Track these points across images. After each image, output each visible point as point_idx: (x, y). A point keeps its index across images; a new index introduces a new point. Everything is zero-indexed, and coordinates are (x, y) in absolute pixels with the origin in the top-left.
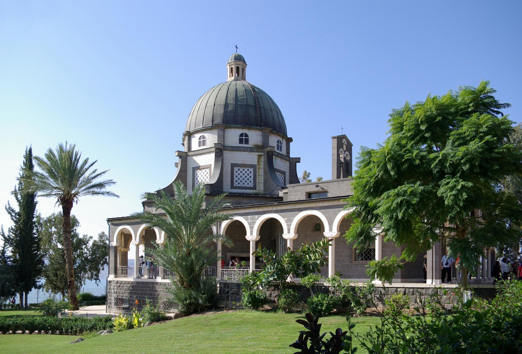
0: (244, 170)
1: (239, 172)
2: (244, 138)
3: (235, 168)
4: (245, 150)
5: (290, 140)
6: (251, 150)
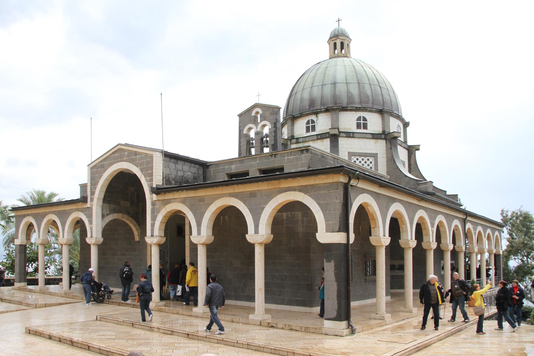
4: (364, 136)
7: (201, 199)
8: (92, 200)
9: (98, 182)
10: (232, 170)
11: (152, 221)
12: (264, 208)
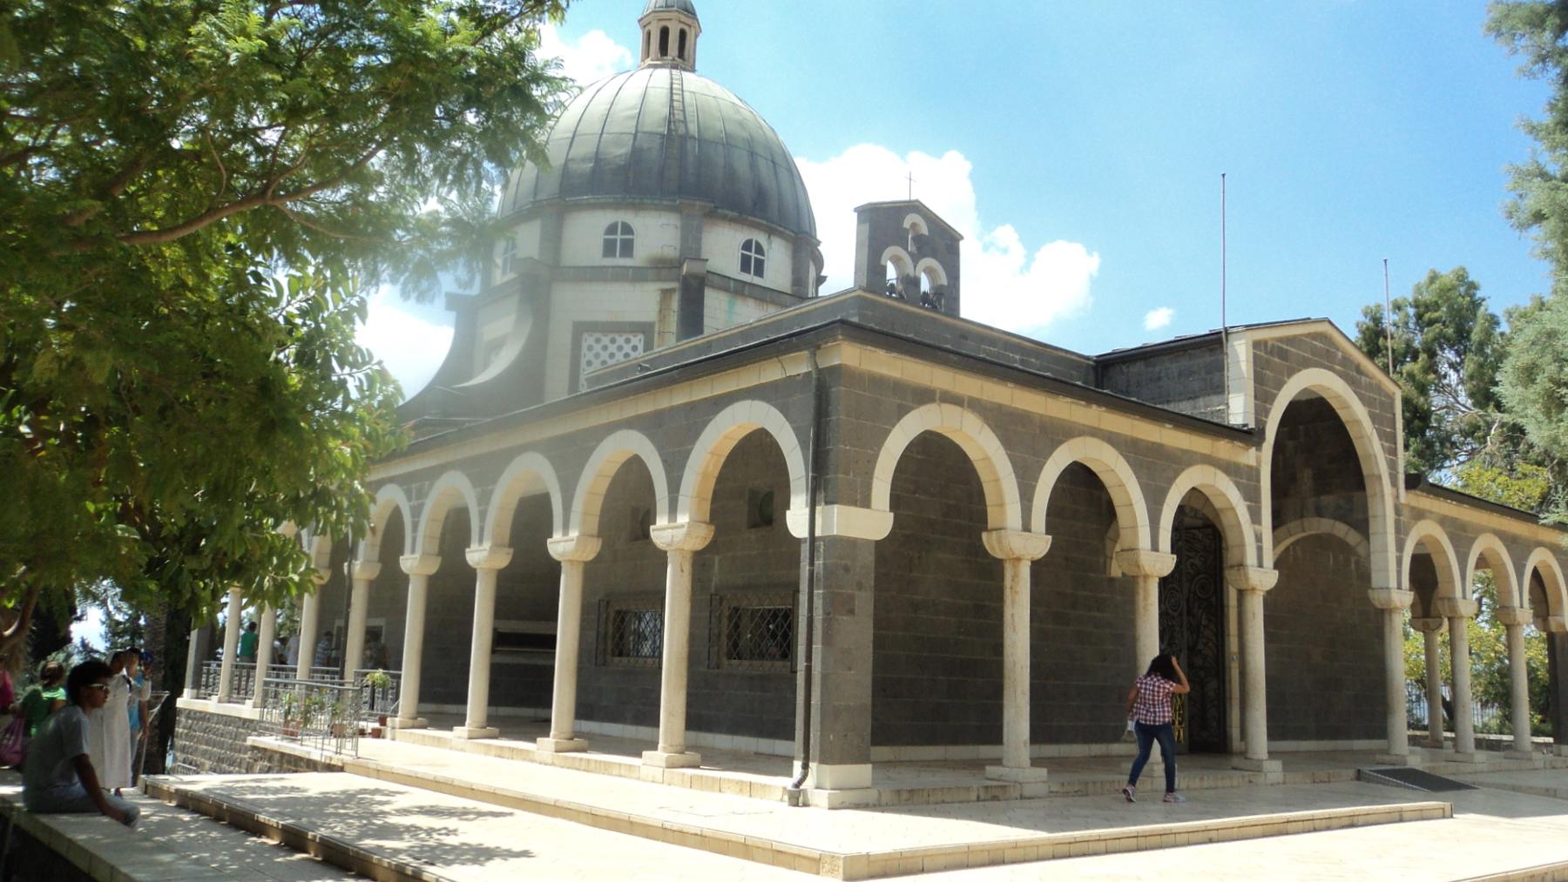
0: (613, 341)
1: (598, 348)
2: (619, 237)
3: (585, 335)
6: (637, 276)
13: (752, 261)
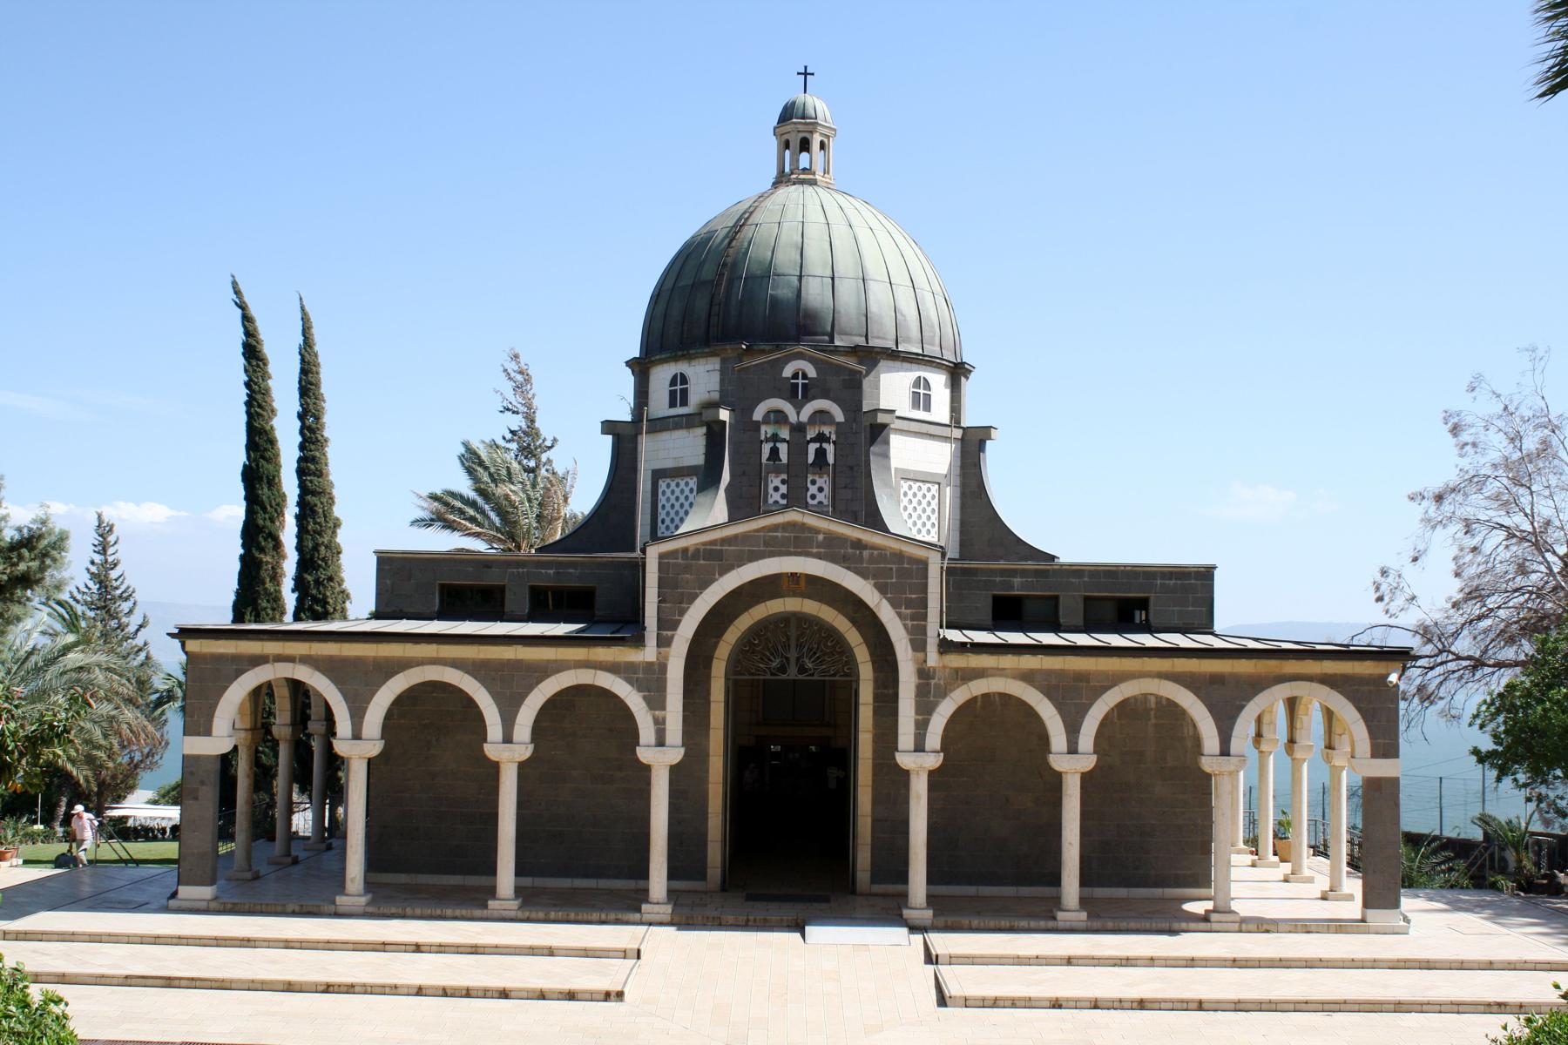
3: (771, 477)
5: (957, 372)
7: (1082, 677)
8: (664, 642)
9: (692, 598)
10: (1012, 588)
11: (917, 713)
12: (1242, 707)
13: (921, 399)
